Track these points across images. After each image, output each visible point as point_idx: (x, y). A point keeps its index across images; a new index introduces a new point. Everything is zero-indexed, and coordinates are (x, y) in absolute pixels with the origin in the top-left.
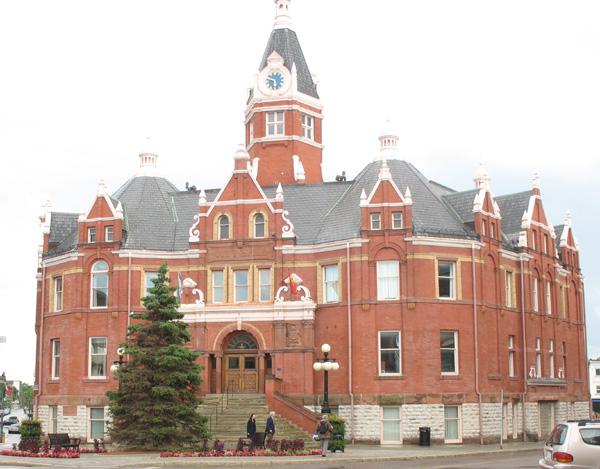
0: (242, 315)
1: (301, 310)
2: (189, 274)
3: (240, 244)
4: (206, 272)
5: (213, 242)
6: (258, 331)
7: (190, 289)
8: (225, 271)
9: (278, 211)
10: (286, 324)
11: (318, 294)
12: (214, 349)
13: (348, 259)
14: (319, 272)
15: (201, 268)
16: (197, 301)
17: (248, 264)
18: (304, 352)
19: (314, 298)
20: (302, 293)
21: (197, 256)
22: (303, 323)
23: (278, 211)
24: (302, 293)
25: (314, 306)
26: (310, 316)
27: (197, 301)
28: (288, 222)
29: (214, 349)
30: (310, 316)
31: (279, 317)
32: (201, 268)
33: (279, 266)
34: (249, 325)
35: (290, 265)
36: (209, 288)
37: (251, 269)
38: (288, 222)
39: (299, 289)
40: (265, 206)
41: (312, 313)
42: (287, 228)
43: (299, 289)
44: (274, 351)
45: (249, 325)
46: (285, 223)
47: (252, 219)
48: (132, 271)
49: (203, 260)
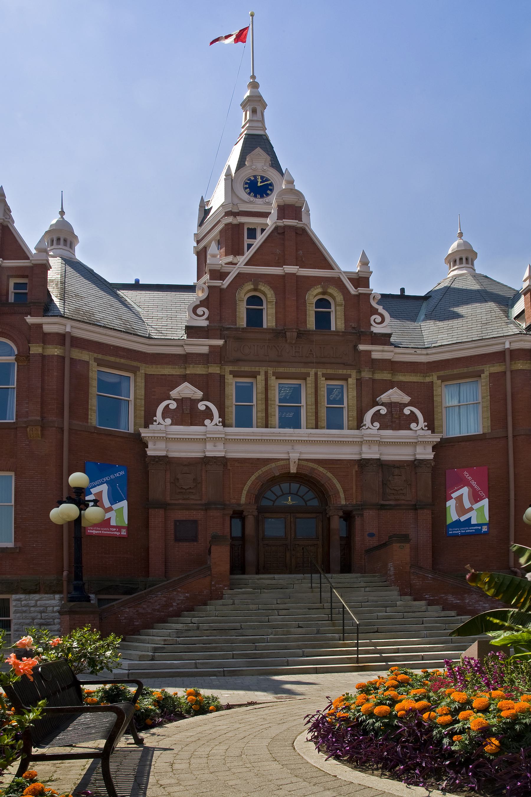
0: (300, 448)
1: (413, 444)
2: (185, 378)
3: (291, 335)
4: (222, 378)
5: (237, 329)
6: (329, 475)
7: (194, 402)
8: (261, 378)
9: (362, 290)
10: (379, 464)
11: (436, 423)
12: (243, 500)
13: (497, 368)
14: (437, 391)
15: (214, 369)
16: (207, 422)
17: (304, 370)
18: (415, 508)
19: (431, 426)
20: (413, 418)
21: (205, 350)
22: (416, 464)
23: (362, 290)
24: (413, 418)
25: (436, 438)
26: (427, 454)
27: (207, 422)
28: (380, 309)
29: (243, 500)
30: (427, 454)
31: (370, 453)
32: (214, 369)
33: (366, 375)
34: (311, 465)
35: (386, 376)
36: (227, 403)
37: (311, 380)
38: (380, 309)
39: (407, 411)
40: (337, 282)
41: (430, 449)
42: (379, 319)
43: (407, 411)
44: (362, 507)
45: (311, 465)
46: (375, 312)
47: (312, 296)
48: (71, 359)
49: (216, 356)
